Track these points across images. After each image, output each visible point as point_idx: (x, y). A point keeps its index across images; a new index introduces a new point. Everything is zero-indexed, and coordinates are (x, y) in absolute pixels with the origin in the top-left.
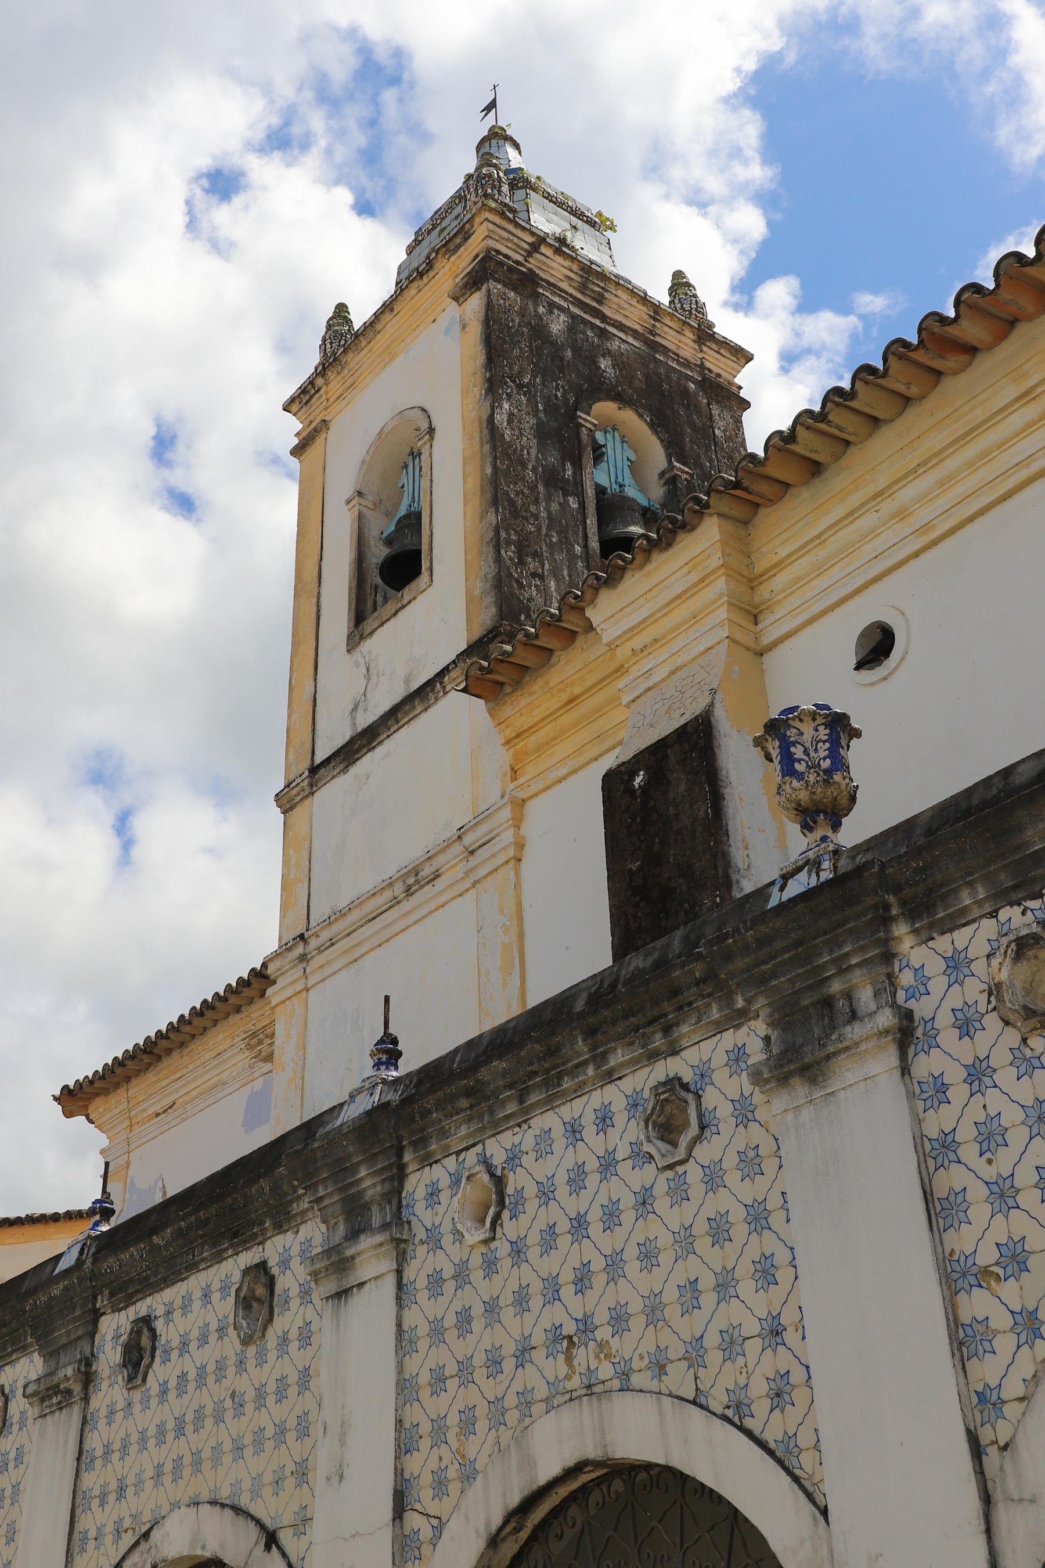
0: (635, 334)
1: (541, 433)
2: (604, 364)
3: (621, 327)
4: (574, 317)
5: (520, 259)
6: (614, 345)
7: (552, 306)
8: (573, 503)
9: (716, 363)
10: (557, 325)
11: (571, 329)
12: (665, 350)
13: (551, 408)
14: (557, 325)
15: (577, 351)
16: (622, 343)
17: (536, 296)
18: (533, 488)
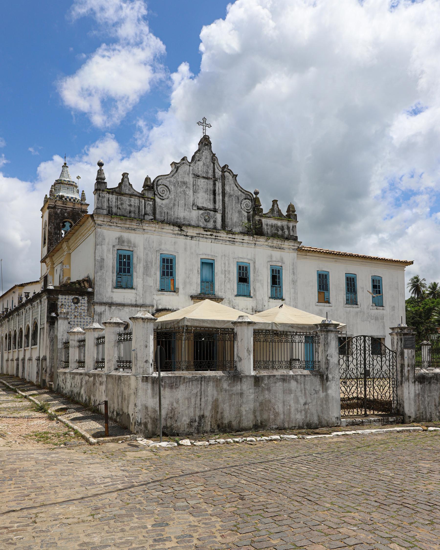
0: (71, 208)
1: (55, 229)
2: (65, 214)
3: (69, 208)
4: (61, 209)
5: (54, 204)
6: (67, 211)
7: (58, 208)
8: (58, 236)
9: (84, 207)
10: (59, 211)
11: (61, 211)
12: (75, 208)
13: (57, 224)
14: (59, 211)
15: (61, 214)
16: (69, 209)
17: (56, 208)
18: (53, 236)
